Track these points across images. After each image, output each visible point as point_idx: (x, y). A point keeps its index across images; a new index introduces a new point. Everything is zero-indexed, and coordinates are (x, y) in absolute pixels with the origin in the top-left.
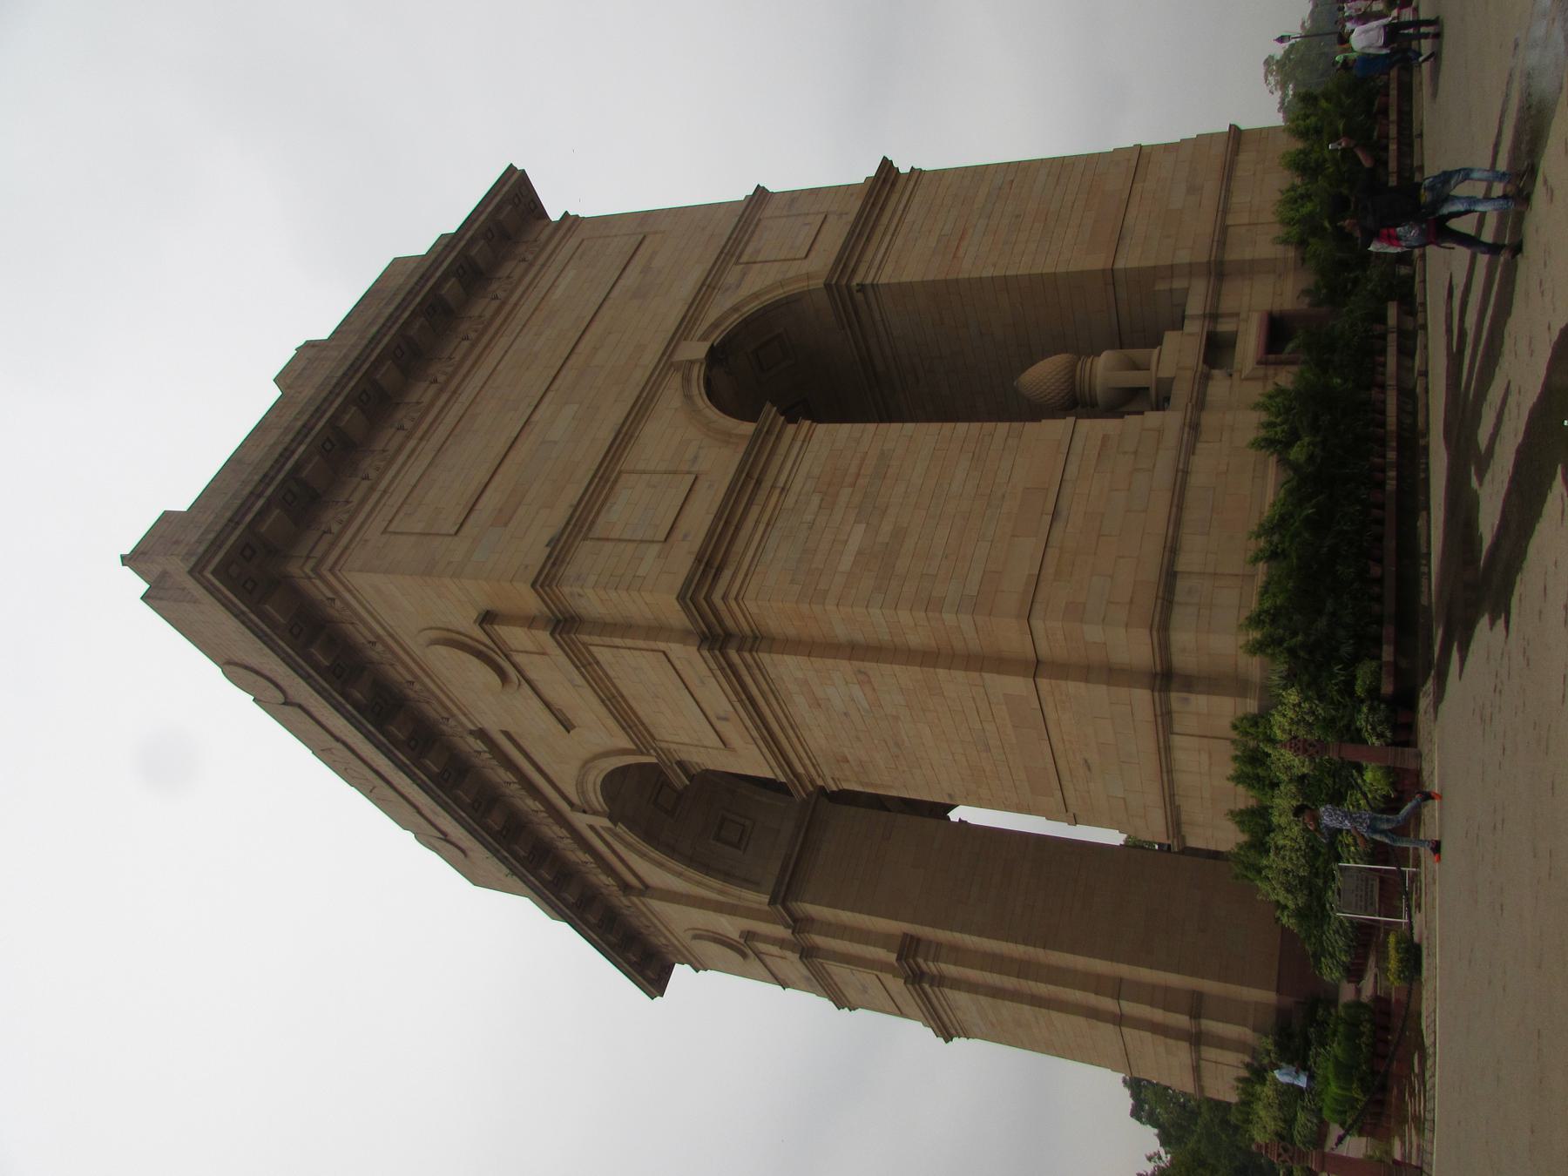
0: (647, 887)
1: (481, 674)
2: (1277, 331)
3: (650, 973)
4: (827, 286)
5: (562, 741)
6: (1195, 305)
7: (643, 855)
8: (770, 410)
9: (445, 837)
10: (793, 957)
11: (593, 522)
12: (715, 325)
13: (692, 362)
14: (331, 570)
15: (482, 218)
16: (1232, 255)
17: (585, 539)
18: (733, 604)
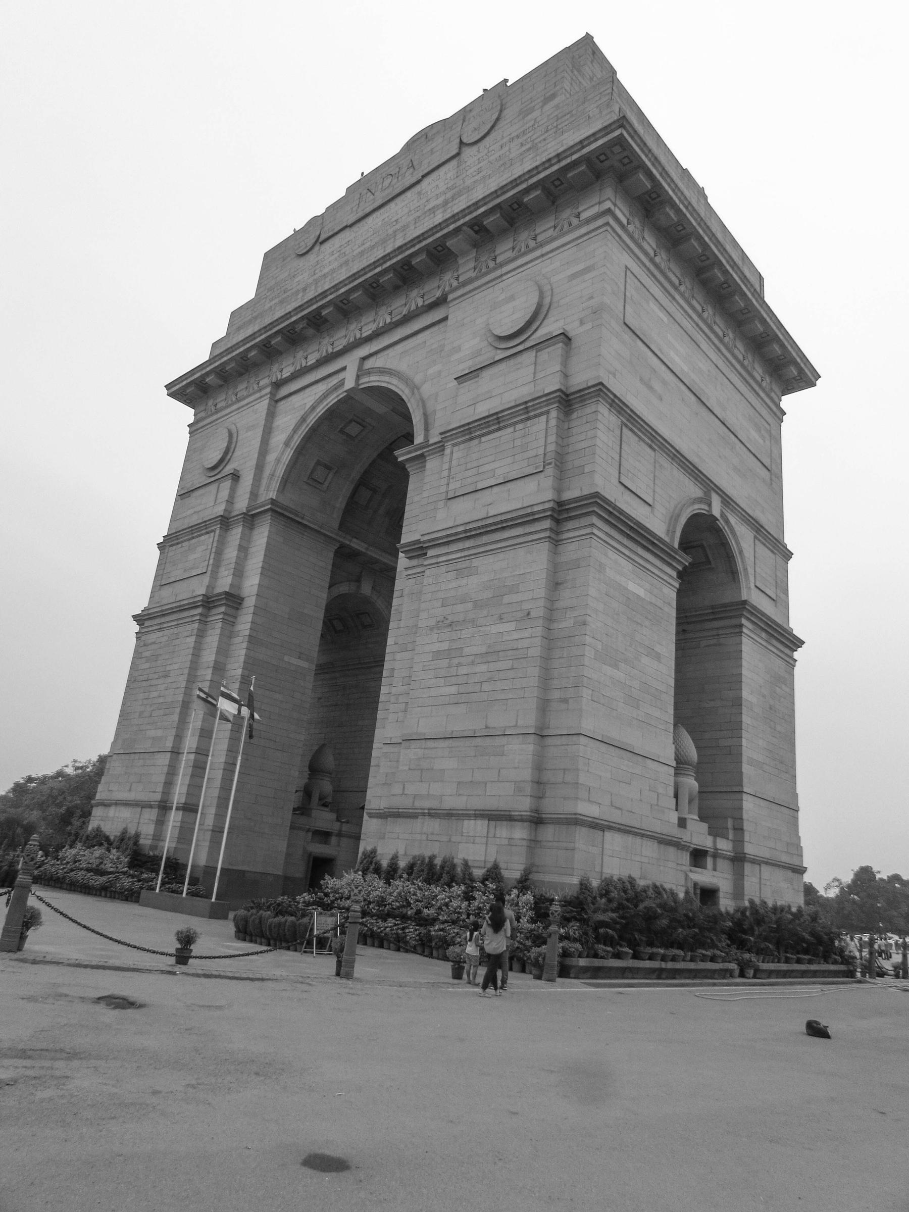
0: (277, 401)
1: (509, 319)
2: (708, 894)
3: (191, 389)
4: (745, 602)
5: (434, 365)
6: (724, 845)
7: (313, 408)
8: (686, 560)
9: (320, 241)
10: (220, 510)
11: (631, 430)
12: (727, 522)
13: (710, 505)
14: (607, 224)
15: (794, 354)
16: (748, 867)
17: (622, 422)
18: (588, 531)
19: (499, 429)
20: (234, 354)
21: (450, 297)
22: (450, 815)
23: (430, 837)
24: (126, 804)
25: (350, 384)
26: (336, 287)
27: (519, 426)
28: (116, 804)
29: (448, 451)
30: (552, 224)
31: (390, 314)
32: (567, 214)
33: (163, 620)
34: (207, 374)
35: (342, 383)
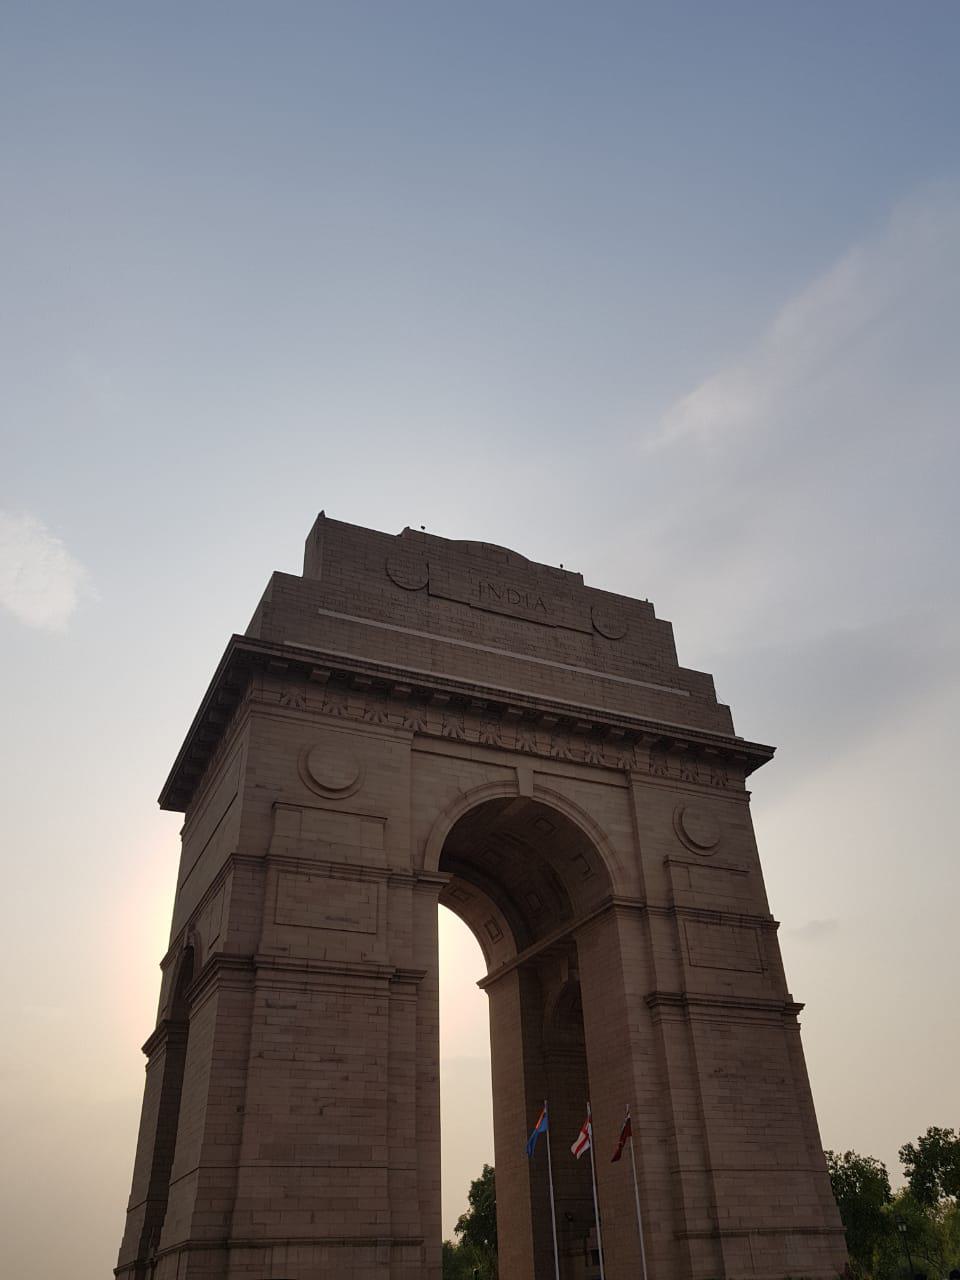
7: (477, 790)
19: (720, 924)
20: (380, 675)
21: (633, 776)
22: (774, 1232)
23: (763, 1251)
24: (315, 1243)
25: (526, 790)
26: (536, 701)
27: (737, 930)
28: (288, 1243)
29: (680, 923)
30: (709, 773)
31: (570, 750)
32: (719, 772)
33: (304, 978)
34: (320, 667)
35: (516, 784)
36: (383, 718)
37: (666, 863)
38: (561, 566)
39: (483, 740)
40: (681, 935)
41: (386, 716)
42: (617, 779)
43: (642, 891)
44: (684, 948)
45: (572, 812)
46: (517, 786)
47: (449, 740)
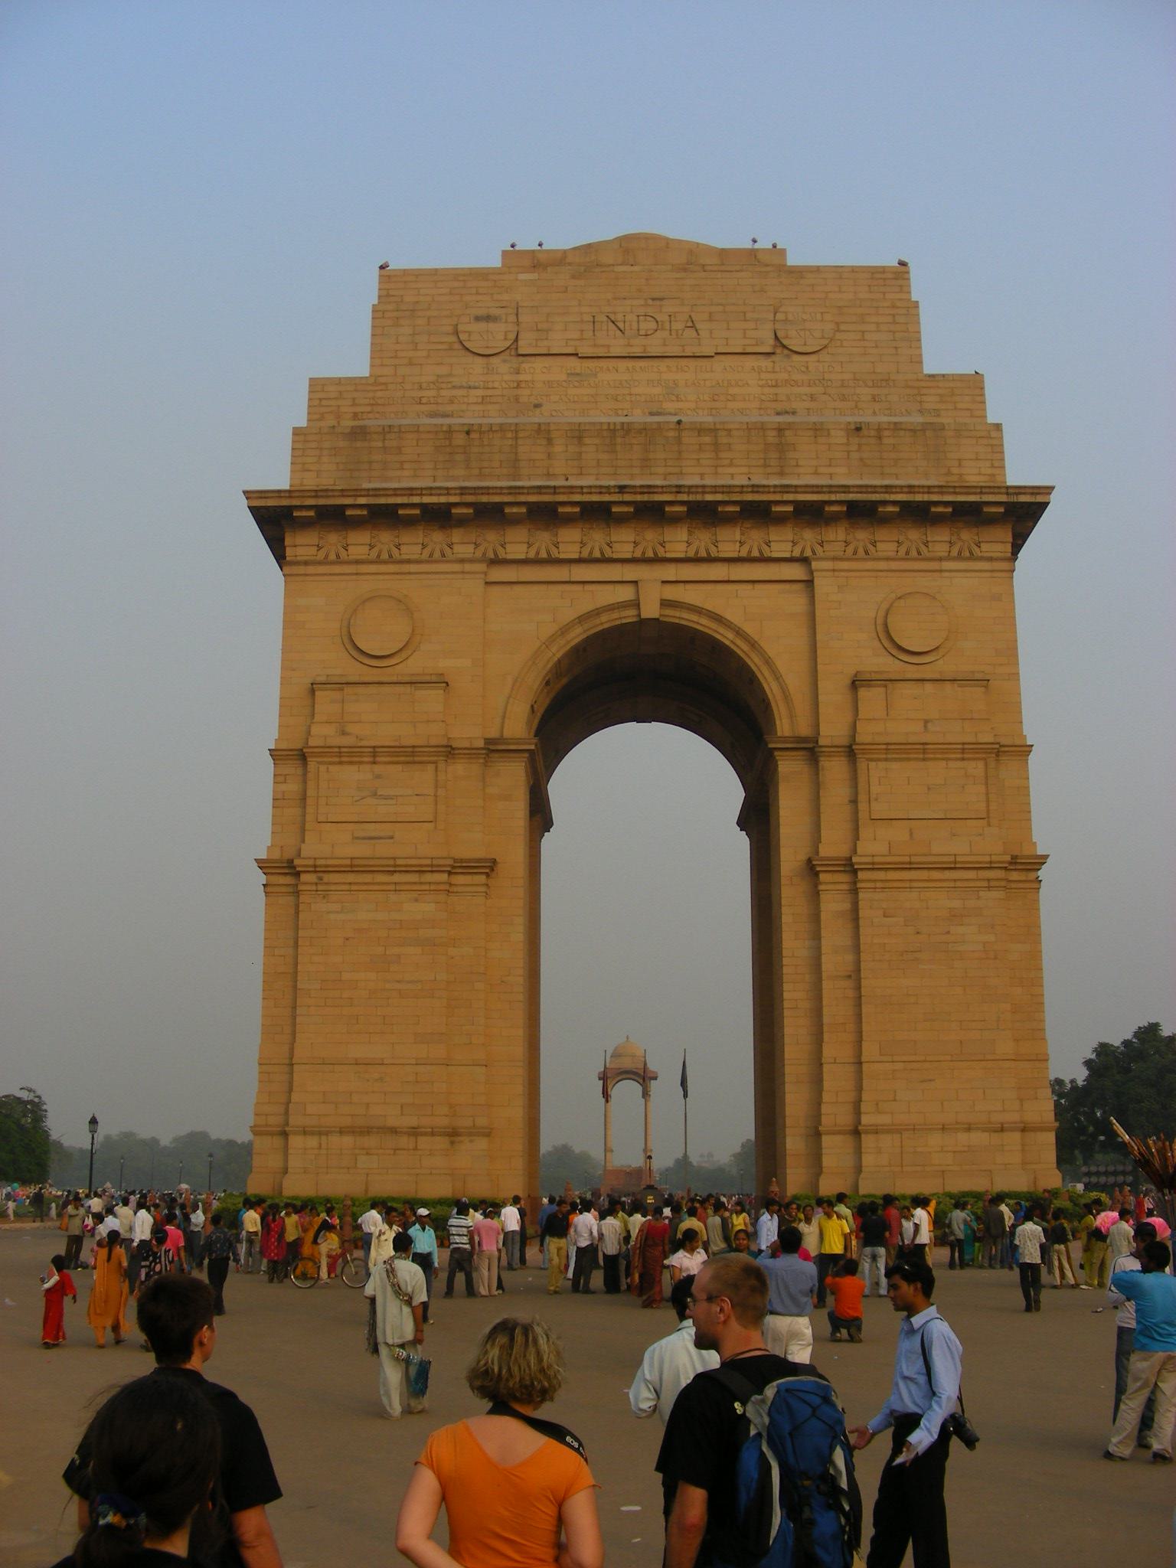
20: (426, 500)
21: (814, 565)
25: (651, 610)
27: (952, 764)
29: (862, 765)
30: (947, 538)
35: (636, 604)
36: (447, 551)
37: (853, 682)
38: (755, 241)
39: (585, 554)
40: (862, 780)
41: (450, 546)
42: (796, 572)
43: (817, 726)
44: (862, 797)
45: (721, 630)
46: (638, 606)
47: (537, 561)
